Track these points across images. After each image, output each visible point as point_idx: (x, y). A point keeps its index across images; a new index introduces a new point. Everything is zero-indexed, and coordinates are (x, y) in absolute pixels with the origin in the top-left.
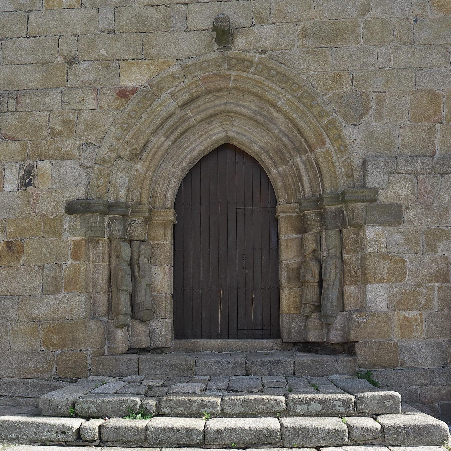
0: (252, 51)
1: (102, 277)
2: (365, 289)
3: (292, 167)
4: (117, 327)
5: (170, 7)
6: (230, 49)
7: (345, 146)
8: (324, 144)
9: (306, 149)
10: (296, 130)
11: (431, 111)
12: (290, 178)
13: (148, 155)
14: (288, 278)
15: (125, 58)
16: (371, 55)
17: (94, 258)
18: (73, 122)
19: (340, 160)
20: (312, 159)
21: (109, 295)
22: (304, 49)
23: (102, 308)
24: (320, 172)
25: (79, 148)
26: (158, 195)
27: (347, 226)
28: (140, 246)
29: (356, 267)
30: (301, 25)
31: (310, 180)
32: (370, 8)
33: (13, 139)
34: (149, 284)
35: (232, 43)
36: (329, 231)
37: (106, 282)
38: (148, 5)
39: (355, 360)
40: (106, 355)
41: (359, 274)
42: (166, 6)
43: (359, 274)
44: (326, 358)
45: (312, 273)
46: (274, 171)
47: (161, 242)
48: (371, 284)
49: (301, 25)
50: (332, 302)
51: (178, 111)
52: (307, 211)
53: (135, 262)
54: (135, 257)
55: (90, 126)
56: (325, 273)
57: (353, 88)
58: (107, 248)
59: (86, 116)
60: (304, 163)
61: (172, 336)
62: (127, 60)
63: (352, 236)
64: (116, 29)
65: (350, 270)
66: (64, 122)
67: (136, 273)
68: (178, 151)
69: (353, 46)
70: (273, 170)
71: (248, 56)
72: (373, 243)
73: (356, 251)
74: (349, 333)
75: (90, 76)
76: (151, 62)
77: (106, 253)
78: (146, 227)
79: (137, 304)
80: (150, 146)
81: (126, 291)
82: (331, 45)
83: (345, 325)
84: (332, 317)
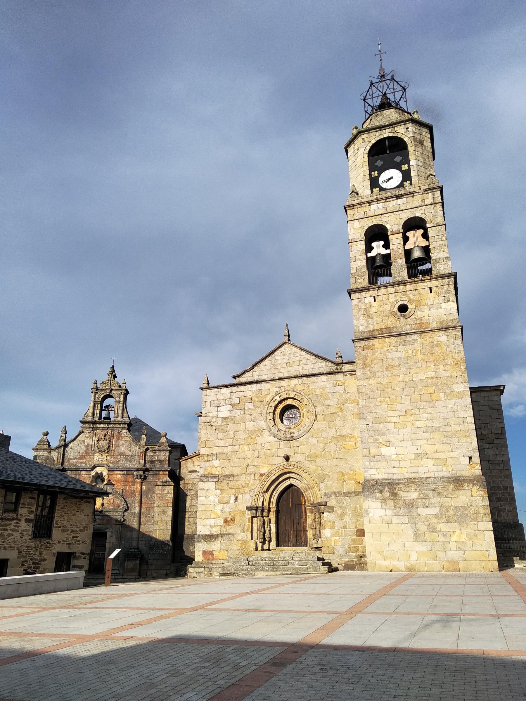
11: (342, 478)
30: (307, 454)
33: (233, 489)
39: (322, 552)
55: (252, 484)
59: (252, 482)
71: (294, 463)
75: (252, 470)
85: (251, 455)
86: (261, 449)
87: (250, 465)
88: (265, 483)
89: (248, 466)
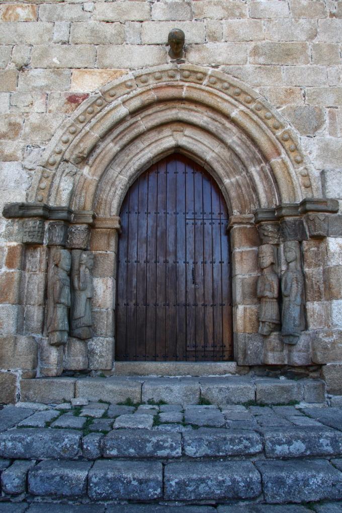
0: (205, 65)
1: (38, 288)
2: (331, 306)
3: (245, 178)
4: (52, 345)
5: (124, 24)
6: (184, 62)
7: (302, 156)
8: (279, 154)
9: (261, 160)
10: (250, 141)
12: (243, 189)
13: (95, 160)
14: (244, 294)
15: (78, 66)
16: (321, 74)
17: (31, 267)
18: (20, 124)
19: (297, 170)
20: (267, 169)
21: (44, 309)
22: (256, 66)
23: (36, 323)
24: (276, 181)
25: (23, 149)
26: (103, 202)
27: (307, 238)
28: (81, 255)
29: (318, 282)
31: (265, 190)
32: (317, 33)
34: (89, 297)
35: (185, 57)
36: (289, 243)
37: (41, 293)
38: (104, 21)
39: (323, 385)
40: (38, 378)
41: (322, 289)
42: (121, 23)
43: (322, 289)
44: (291, 384)
45: (271, 288)
46: (227, 181)
47: (104, 252)
48: (338, 299)
49: (253, 44)
50: (295, 320)
51: (129, 118)
52: (264, 222)
53: (75, 273)
54: (76, 267)
55: (36, 129)
56: (285, 288)
57: (306, 102)
58: (45, 255)
60: (258, 173)
61: (113, 357)
62: (80, 68)
63: (313, 249)
64: (70, 41)
65: (312, 285)
66: (10, 124)
67: (76, 284)
68: (126, 158)
69: (303, 66)
70: (225, 180)
71: (202, 68)
72: (337, 256)
73: (317, 265)
74: (315, 354)
75: (42, 82)
76: (103, 70)
77: (44, 262)
78: (88, 234)
79: (76, 319)
80: (98, 151)
81: (63, 304)
82: (283, 63)
83: (309, 345)
84: (294, 336)
85: (41, 36)
86: (79, 20)
87: (32, 65)
88: (87, 128)
89: (21, 69)
